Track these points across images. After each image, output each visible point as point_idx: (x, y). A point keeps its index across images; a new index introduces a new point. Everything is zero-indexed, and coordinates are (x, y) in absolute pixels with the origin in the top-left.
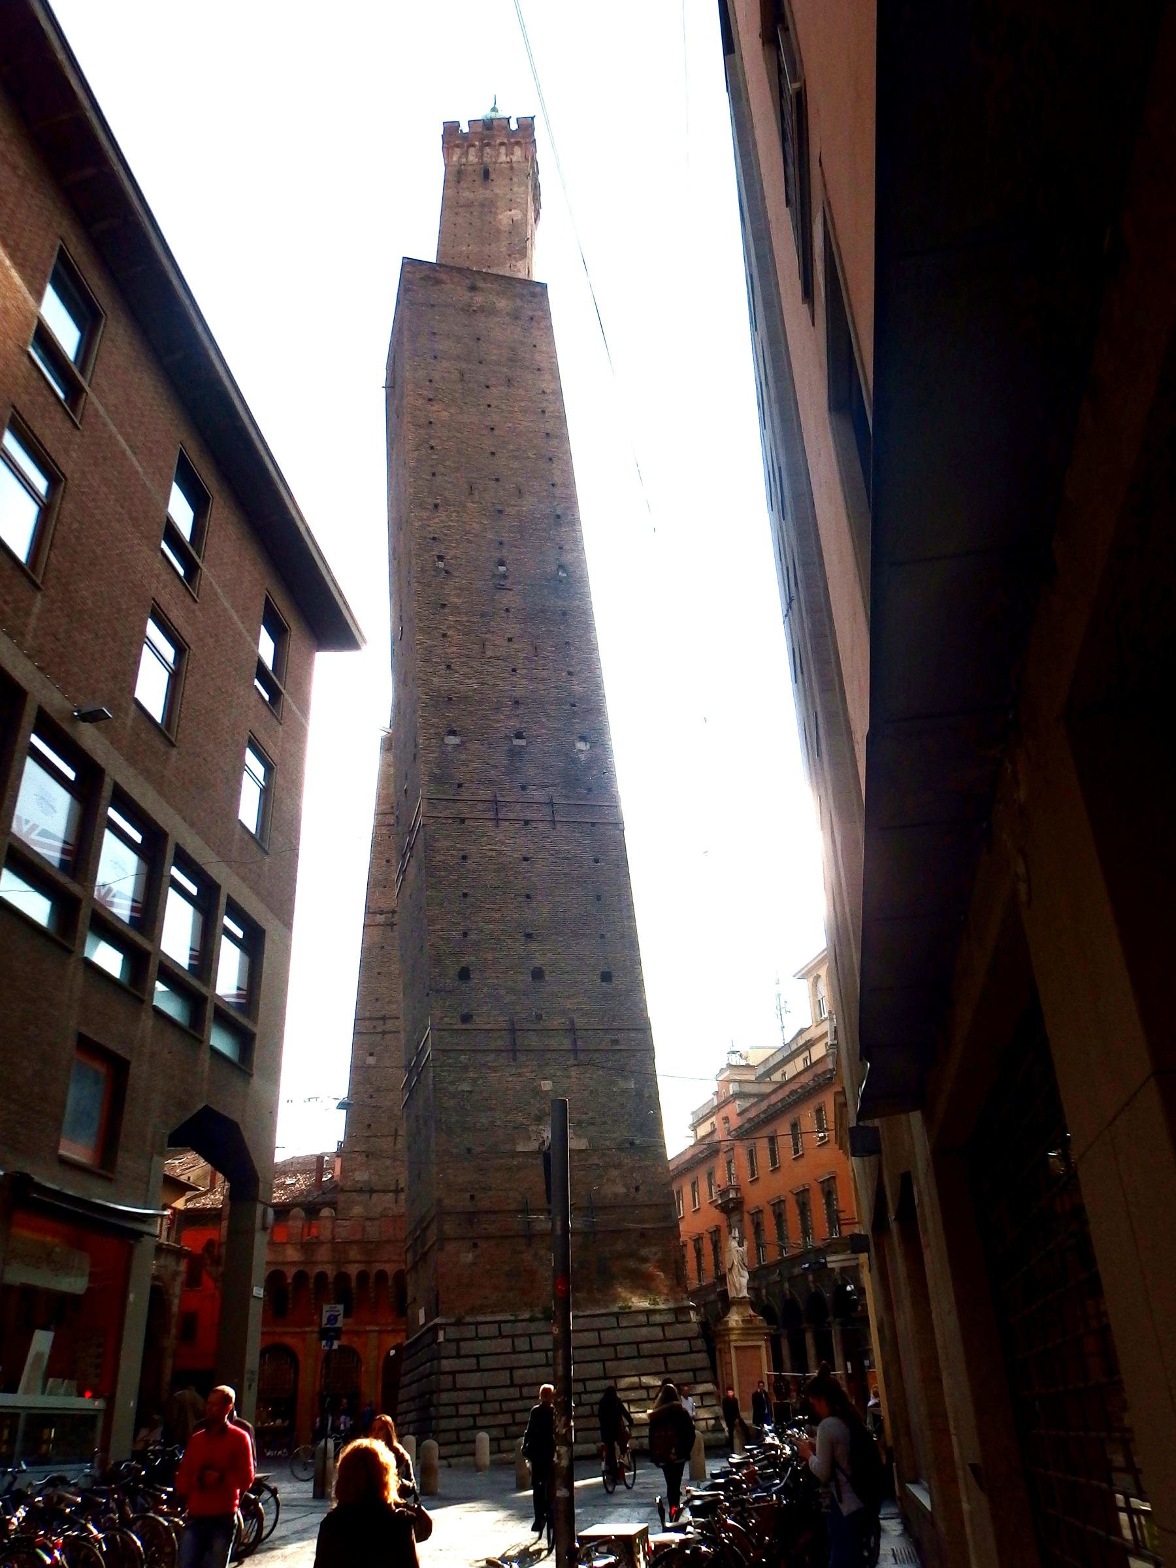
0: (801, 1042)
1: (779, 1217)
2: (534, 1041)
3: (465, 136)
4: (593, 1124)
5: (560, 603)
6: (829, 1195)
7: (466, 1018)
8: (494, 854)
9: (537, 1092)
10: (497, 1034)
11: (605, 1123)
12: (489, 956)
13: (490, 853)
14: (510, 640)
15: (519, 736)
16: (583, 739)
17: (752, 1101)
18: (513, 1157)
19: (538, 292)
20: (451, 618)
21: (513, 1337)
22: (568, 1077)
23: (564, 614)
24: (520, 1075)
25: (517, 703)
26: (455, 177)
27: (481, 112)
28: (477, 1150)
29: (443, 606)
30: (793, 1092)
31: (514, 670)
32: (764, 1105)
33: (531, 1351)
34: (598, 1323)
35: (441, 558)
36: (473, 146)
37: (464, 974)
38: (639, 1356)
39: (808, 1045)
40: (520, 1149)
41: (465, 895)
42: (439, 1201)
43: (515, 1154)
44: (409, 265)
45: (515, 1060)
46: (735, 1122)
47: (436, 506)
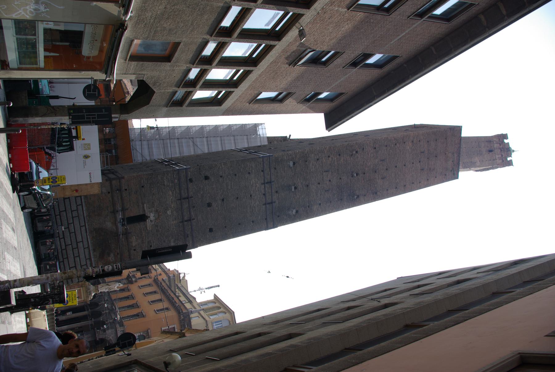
0: (191, 299)
1: (127, 298)
3: (503, 142)
5: (345, 198)
6: (137, 315)
7: (191, 180)
12: (214, 186)
14: (330, 181)
15: (295, 188)
16: (297, 212)
17: (168, 284)
19: (455, 176)
21: (77, 210)
23: (341, 200)
25: (307, 186)
26: (488, 140)
27: (512, 146)
29: (340, 155)
30: (173, 298)
31: (319, 183)
32: (166, 288)
33: (73, 218)
34: (85, 240)
35: (357, 152)
37: (207, 178)
38: (74, 257)
39: (190, 302)
40: (145, 205)
41: (236, 175)
42: (123, 178)
43: (143, 204)
44: (458, 129)
46: (160, 278)
47: (375, 148)
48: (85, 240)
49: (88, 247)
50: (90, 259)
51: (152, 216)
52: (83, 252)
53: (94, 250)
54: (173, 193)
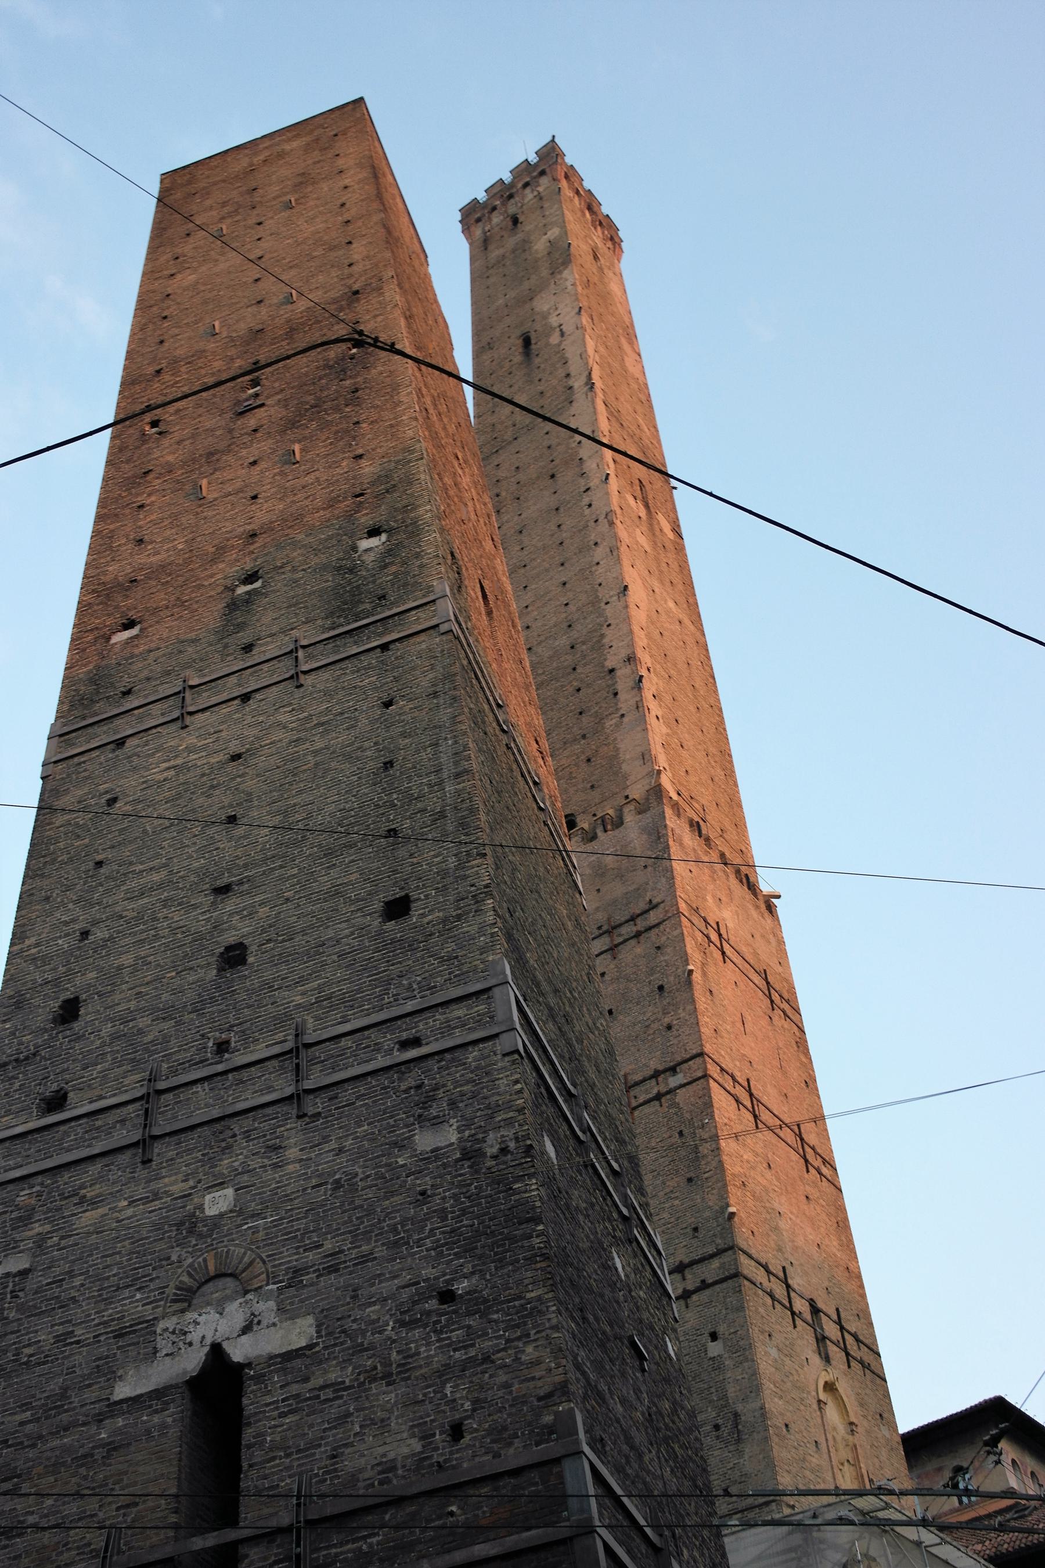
4: (333, 1269)
8: (172, 773)
9: (192, 1226)
10: (111, 1117)
11: (365, 1259)
12: (127, 960)
14: (254, 463)
20: (158, 481)
22: (276, 1166)
24: (156, 1196)
31: (255, 497)
36: (494, 208)
40: (122, 1391)
41: (99, 864)
43: (115, 1408)
45: (146, 1162)
51: (215, 1324)
54: (94, 1203)
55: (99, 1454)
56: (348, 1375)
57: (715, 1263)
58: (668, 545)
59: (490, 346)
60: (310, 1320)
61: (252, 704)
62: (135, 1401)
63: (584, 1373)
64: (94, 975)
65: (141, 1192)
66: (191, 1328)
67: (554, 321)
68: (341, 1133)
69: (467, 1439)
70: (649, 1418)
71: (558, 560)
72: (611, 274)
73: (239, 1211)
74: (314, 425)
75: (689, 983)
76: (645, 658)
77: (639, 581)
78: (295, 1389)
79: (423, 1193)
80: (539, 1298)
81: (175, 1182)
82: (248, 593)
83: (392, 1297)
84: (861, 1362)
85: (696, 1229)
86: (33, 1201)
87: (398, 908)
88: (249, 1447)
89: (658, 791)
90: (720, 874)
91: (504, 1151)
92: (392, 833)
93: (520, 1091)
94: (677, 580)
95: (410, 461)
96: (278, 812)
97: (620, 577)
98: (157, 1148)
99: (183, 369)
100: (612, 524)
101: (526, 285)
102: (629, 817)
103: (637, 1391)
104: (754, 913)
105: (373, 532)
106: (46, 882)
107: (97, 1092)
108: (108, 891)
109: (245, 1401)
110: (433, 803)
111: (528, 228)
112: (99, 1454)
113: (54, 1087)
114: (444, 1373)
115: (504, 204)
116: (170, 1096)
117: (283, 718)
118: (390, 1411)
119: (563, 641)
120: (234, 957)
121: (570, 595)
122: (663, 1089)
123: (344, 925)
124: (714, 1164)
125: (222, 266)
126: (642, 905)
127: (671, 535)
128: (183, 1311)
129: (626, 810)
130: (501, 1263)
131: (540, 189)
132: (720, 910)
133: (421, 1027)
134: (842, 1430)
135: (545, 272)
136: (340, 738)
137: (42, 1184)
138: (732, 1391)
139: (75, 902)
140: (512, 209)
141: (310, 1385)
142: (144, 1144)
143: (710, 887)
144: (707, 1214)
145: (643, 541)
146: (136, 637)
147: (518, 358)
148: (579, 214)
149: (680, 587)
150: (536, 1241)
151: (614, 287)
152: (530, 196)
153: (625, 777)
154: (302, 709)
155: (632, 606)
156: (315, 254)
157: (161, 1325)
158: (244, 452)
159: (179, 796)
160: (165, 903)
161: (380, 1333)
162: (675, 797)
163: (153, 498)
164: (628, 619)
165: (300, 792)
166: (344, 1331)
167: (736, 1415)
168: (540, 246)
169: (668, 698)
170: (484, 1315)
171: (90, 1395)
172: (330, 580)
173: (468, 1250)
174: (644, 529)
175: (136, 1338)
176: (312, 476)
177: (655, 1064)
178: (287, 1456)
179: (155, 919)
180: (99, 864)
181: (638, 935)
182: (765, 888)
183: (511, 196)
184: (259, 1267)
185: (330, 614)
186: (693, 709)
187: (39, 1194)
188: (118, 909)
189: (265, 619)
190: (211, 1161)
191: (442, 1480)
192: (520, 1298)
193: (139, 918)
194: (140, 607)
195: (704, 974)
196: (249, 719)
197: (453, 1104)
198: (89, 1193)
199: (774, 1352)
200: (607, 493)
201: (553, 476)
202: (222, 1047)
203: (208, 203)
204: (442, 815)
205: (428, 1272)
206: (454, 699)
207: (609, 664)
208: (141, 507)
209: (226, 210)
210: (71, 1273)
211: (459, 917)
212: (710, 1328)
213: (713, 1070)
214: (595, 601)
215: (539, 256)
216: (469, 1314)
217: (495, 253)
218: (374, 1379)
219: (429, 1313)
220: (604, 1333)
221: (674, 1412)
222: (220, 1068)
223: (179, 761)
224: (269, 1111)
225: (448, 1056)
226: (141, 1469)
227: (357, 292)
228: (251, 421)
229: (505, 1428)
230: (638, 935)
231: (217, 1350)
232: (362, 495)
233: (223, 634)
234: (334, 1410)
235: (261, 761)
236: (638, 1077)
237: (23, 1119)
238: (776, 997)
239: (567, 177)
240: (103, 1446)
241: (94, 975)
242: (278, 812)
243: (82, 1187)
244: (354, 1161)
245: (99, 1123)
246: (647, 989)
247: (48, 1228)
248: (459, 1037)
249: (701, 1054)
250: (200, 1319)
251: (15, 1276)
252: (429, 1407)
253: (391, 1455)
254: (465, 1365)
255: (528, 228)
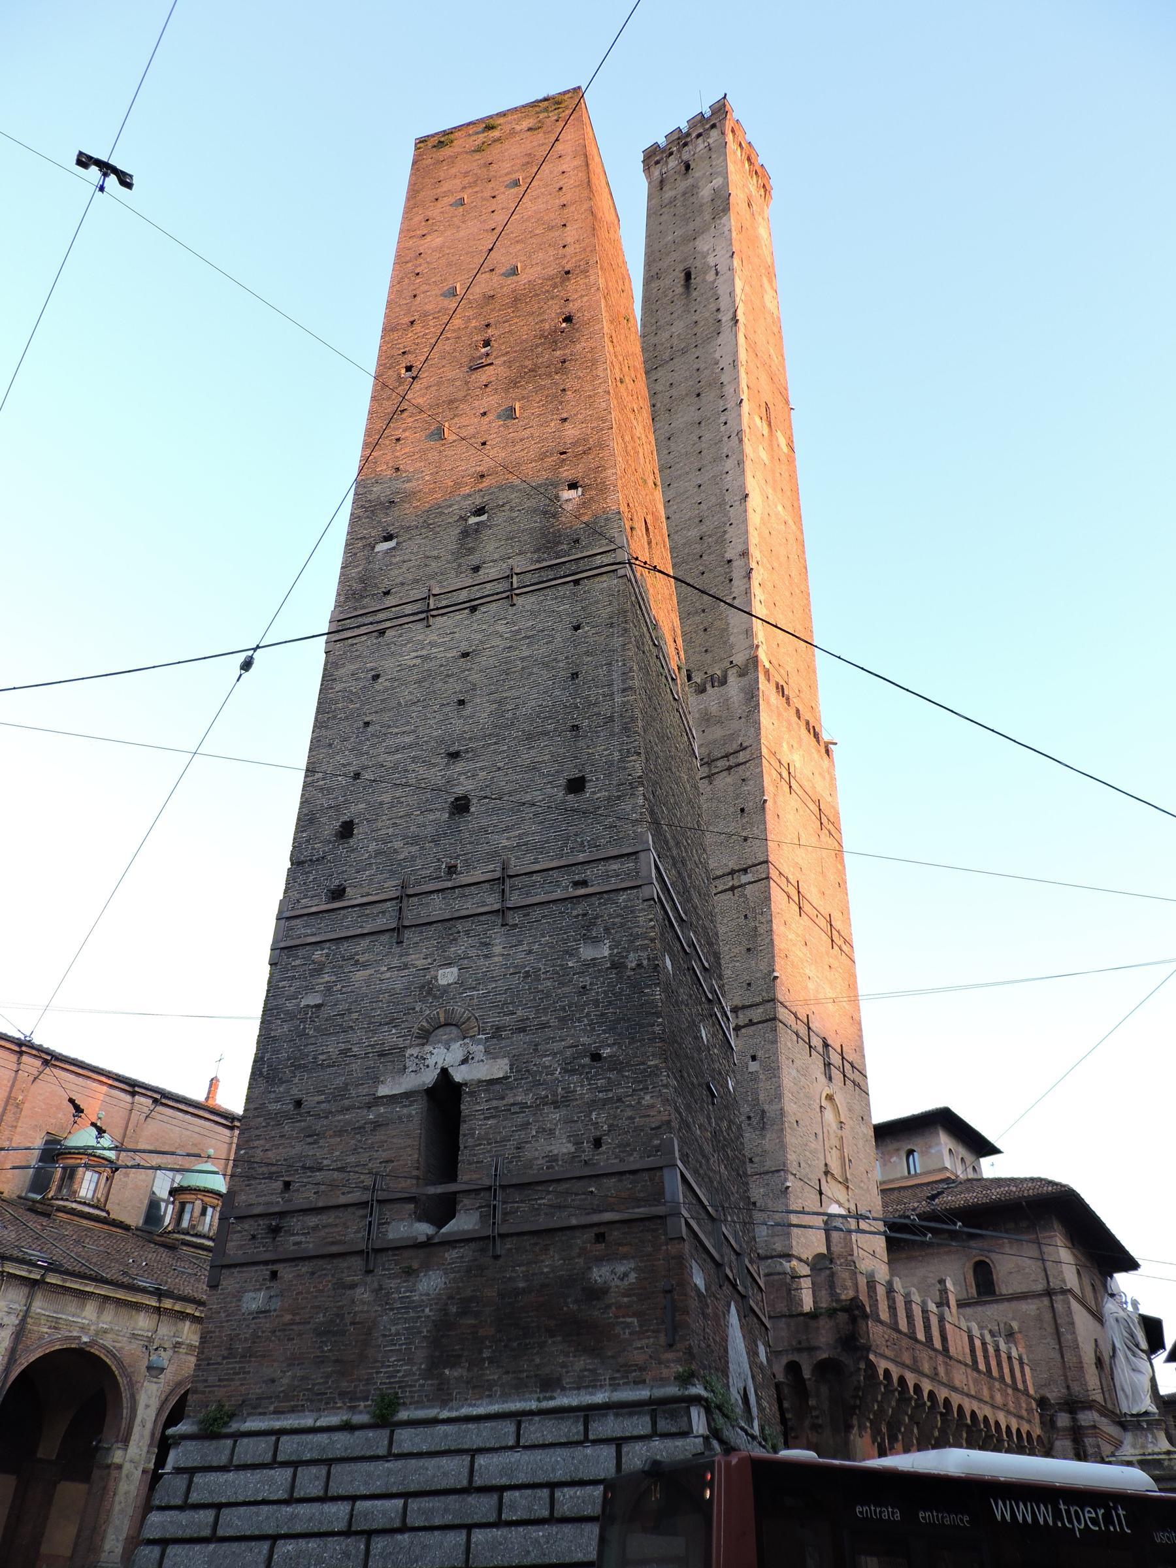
2: (437, 908)
4: (523, 1030)
7: (338, 893)
8: (419, 661)
9: (429, 990)
11: (544, 1026)
12: (386, 798)
13: (414, 661)
14: (484, 414)
15: (480, 511)
18: (369, 1107)
22: (486, 956)
24: (406, 966)
26: (659, 186)
28: (310, 1101)
31: (484, 444)
34: (475, 1436)
36: (671, 154)
40: (383, 1091)
41: (367, 724)
43: (378, 1101)
45: (399, 943)
48: (475, 1436)
49: (518, 1417)
50: (588, 1412)
51: (445, 1055)
52: (538, 1455)
53: (549, 1384)
54: (365, 966)
55: (368, 1127)
56: (529, 1099)
57: (760, 1010)
58: (783, 458)
59: (658, 276)
60: (506, 1061)
61: (478, 615)
62: (392, 1099)
63: (680, 1113)
64: (363, 806)
65: (396, 963)
66: (428, 1056)
67: (711, 261)
68: (531, 940)
69: (604, 1148)
70: (715, 1134)
71: (697, 465)
72: (760, 219)
73: (460, 983)
74: (531, 386)
75: (764, 809)
76: (755, 553)
77: (758, 490)
78: (494, 1103)
79: (584, 987)
80: (656, 1066)
81: (418, 959)
82: (477, 524)
83: (560, 1052)
84: (853, 1082)
85: (749, 984)
86: (323, 959)
87: (576, 785)
88: (464, 1135)
89: (754, 661)
90: (795, 726)
91: (640, 965)
92: (575, 728)
93: (653, 927)
94: (787, 488)
95: (602, 430)
96: (495, 702)
97: (743, 486)
98: (407, 934)
99: (431, 323)
100: (741, 441)
101: (692, 225)
102: (732, 679)
103: (709, 1118)
104: (816, 755)
105: (573, 486)
106: (329, 732)
107: (366, 890)
108: (373, 745)
109: (462, 1107)
110: (605, 709)
111: (697, 175)
112: (368, 1127)
113: (337, 882)
114: (593, 1104)
115: (679, 151)
116: (416, 899)
117: (501, 628)
118: (556, 1125)
119: (694, 533)
120: (461, 806)
121: (703, 495)
122: (736, 883)
123: (539, 793)
124: (767, 941)
125: (462, 233)
126: (735, 746)
127: (785, 449)
128: (423, 1045)
129: (730, 673)
130: (633, 1040)
131: (711, 141)
132: (791, 753)
133: (588, 873)
134: (834, 1126)
135: (707, 216)
136: (541, 650)
137: (329, 948)
138: (762, 1097)
139: (351, 750)
140: (685, 157)
141: (504, 1102)
142: (398, 931)
143: (786, 736)
144: (758, 975)
145: (764, 455)
146: (394, 548)
147: (680, 290)
148: (740, 165)
149: (789, 493)
150: (657, 1029)
151: (762, 232)
152: (702, 146)
153: (732, 647)
154: (514, 623)
155: (750, 511)
156: (537, 232)
157: (409, 1052)
158: (477, 403)
159: (424, 679)
160: (414, 759)
161: (552, 1074)
162: (767, 665)
163: (407, 434)
164: (745, 521)
165: (511, 688)
166: (528, 1071)
167: (763, 1112)
168: (706, 192)
169: (769, 585)
170: (620, 1071)
171: (363, 1090)
172: (537, 522)
173: (612, 1029)
174: (765, 445)
175: (391, 1057)
176: (528, 431)
177: (732, 865)
178: (489, 1144)
179: (406, 771)
180: (367, 724)
181: (729, 768)
182: (825, 737)
183: (686, 144)
184: (473, 1023)
185: (537, 550)
186: (787, 594)
187: (328, 955)
188: (380, 759)
189: (489, 547)
190: (442, 948)
191: (587, 1172)
192: (643, 1064)
193: (395, 767)
194: (397, 524)
195: (775, 802)
196: (475, 626)
197: (607, 930)
198: (361, 959)
199: (794, 1073)
200: (740, 415)
201: (698, 395)
202: (452, 870)
203: (453, 171)
204: (611, 719)
205: (584, 1040)
206: (625, 630)
207: (728, 556)
208: (398, 440)
209: (467, 180)
210: (349, 1011)
211: (619, 797)
212: (752, 1052)
213: (774, 874)
214: (722, 504)
215: (705, 201)
216: (610, 1070)
217: (669, 194)
218: (547, 1104)
219: (583, 1066)
220: (693, 1084)
221: (729, 1128)
222: (449, 884)
223: (424, 652)
224: (482, 918)
225: (605, 896)
226: (394, 1140)
227: (568, 273)
228: (483, 376)
229: (628, 1145)
230: (729, 768)
231: (444, 1072)
232: (565, 453)
233: (458, 555)
234: (519, 1119)
235: (484, 661)
236: (719, 873)
237: (316, 902)
238: (824, 820)
239: (733, 131)
240: (372, 1123)
241: (363, 806)
242: (495, 702)
243: (357, 954)
244: (539, 960)
245: (368, 912)
246: (732, 810)
247: (334, 978)
248: (614, 883)
249: (767, 862)
250: (434, 1051)
251: (312, 1007)
252: (580, 1124)
253: (556, 1152)
254: (605, 1102)
255: (697, 175)
